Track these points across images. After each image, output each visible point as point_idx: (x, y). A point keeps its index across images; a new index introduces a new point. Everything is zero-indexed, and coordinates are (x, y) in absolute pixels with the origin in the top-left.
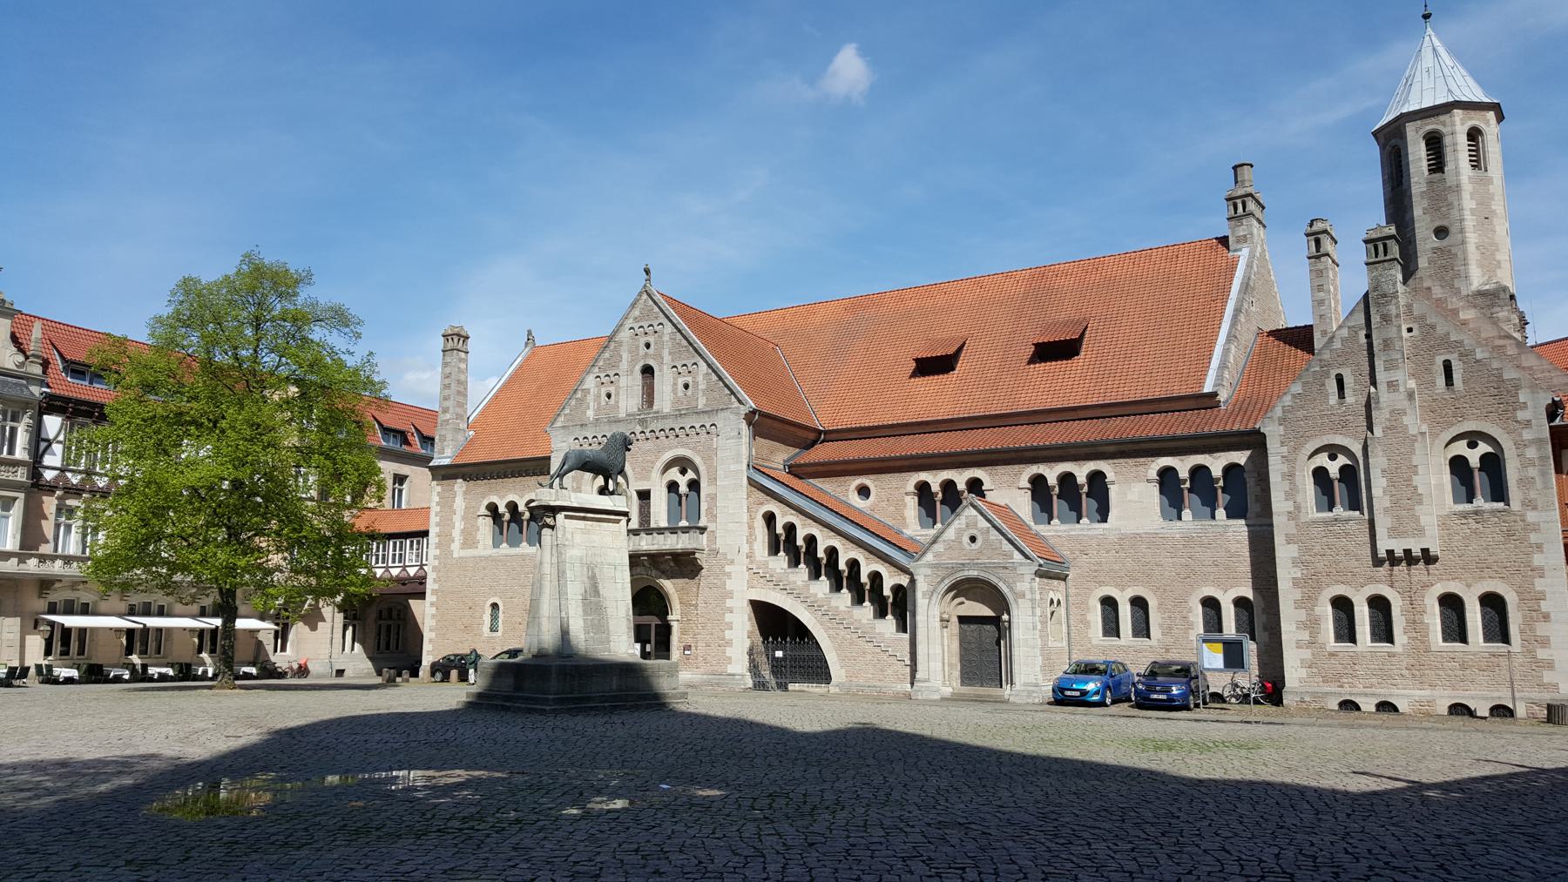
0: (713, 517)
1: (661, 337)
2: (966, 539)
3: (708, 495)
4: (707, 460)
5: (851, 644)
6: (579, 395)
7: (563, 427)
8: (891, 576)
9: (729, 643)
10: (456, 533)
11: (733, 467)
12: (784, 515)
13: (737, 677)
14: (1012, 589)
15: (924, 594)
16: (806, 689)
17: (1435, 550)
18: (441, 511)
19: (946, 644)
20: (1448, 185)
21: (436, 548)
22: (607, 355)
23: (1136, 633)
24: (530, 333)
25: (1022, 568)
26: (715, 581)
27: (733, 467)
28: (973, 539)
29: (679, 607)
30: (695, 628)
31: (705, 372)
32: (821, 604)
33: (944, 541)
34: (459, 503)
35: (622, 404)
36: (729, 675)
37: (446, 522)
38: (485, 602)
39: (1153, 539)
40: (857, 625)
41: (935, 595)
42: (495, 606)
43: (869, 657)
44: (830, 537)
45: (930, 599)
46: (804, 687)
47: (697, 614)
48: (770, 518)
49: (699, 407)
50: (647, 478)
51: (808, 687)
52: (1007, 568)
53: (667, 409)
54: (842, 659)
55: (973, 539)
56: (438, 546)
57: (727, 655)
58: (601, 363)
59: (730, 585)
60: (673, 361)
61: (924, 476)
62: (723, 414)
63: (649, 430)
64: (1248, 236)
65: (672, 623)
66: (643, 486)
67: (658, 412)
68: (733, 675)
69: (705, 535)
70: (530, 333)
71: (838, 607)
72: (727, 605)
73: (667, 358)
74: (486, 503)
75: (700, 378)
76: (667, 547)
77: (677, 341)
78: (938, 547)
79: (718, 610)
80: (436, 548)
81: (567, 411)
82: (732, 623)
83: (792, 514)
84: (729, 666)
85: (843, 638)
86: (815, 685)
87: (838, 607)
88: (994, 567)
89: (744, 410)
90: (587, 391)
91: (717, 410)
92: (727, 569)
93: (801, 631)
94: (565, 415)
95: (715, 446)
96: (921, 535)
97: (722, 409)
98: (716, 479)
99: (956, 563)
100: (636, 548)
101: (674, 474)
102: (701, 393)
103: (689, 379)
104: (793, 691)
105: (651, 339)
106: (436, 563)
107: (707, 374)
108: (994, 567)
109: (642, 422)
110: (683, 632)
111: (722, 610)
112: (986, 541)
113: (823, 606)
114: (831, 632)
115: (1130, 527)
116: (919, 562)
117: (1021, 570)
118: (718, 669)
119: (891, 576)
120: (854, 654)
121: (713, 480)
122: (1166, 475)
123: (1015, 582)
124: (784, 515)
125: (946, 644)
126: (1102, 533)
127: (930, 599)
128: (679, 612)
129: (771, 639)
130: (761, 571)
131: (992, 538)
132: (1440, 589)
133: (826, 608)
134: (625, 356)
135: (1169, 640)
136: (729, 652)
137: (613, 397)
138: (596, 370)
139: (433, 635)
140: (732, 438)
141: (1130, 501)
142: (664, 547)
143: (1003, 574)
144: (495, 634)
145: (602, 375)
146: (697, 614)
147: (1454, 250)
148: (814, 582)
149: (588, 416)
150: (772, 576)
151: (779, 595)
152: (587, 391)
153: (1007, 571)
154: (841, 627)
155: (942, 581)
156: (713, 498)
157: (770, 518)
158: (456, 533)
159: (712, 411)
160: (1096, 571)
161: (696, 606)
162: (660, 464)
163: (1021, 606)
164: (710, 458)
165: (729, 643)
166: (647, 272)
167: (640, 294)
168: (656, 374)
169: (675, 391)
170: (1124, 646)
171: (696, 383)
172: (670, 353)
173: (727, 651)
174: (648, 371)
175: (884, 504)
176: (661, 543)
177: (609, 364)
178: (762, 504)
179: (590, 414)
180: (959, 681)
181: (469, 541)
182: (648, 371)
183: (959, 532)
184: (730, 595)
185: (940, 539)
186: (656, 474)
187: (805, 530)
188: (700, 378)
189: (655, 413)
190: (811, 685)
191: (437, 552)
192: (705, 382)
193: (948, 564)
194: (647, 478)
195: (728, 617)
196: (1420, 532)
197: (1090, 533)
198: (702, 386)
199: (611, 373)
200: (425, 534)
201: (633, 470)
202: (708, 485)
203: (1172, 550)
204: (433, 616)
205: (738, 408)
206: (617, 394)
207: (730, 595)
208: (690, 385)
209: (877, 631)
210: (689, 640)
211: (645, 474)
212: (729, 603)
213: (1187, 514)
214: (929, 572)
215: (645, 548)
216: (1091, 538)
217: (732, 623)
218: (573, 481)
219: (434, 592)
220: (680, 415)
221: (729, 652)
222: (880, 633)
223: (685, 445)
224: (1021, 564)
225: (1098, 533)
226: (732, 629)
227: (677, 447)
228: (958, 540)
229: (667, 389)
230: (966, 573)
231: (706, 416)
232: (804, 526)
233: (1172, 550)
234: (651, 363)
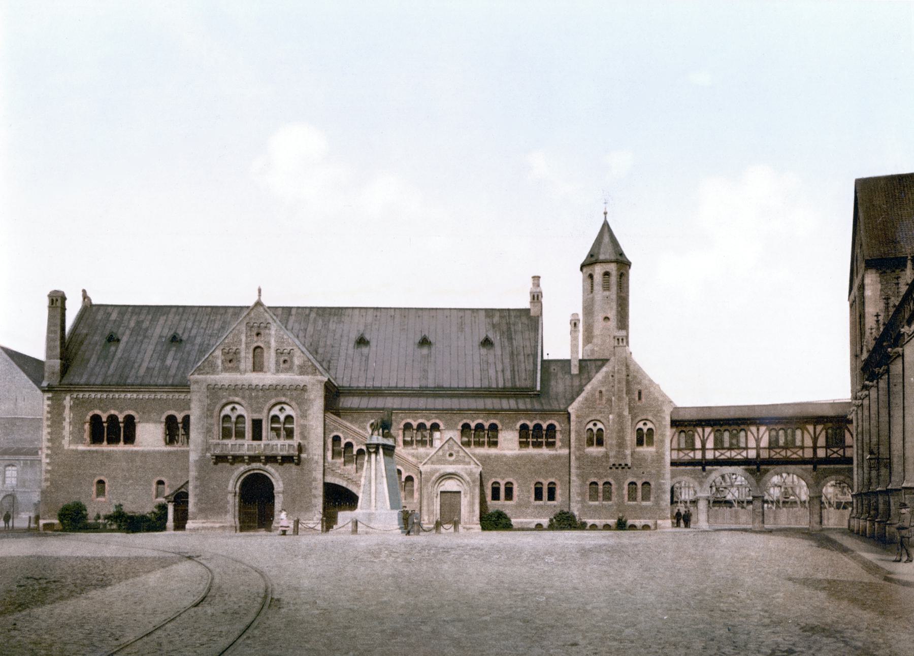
17: (630, 465)
24: (84, 291)
48: (336, 439)
66: (256, 416)
70: (84, 291)
74: (91, 414)
132: (630, 480)
162: (268, 406)
166: (260, 291)
186: (266, 411)
196: (625, 456)
207: (315, 480)
211: (260, 410)
228: (444, 455)
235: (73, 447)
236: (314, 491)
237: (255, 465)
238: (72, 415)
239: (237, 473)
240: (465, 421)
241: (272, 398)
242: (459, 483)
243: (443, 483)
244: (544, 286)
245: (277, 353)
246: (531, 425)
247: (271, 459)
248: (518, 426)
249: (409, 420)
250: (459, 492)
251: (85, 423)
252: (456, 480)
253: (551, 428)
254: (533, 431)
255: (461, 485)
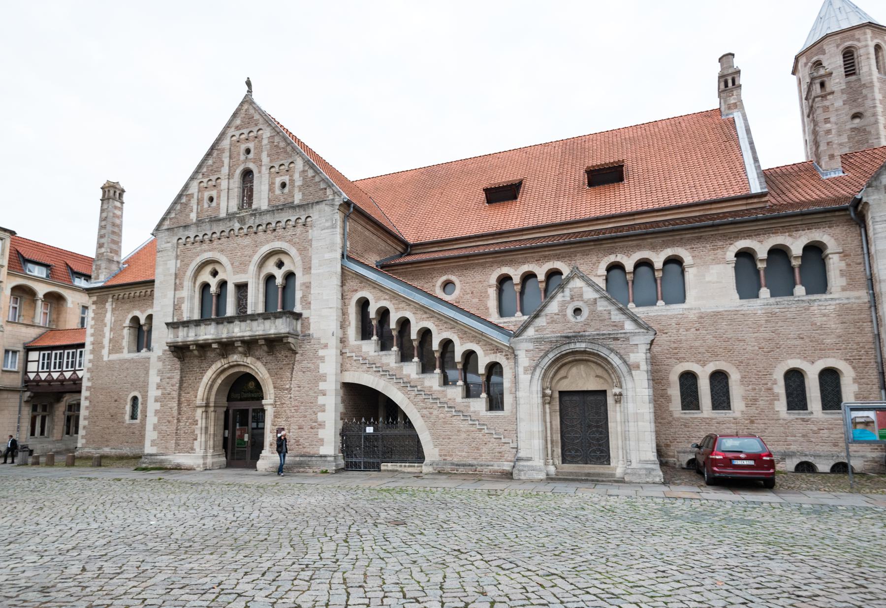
0: (307, 304)
1: (260, 142)
2: (570, 312)
3: (304, 284)
4: (304, 250)
5: (445, 423)
6: (184, 200)
7: (168, 229)
8: (486, 355)
9: (322, 425)
10: (106, 342)
11: (327, 256)
12: (377, 300)
13: (329, 459)
14: (625, 362)
15: (526, 370)
16: (399, 469)
18: (95, 324)
19: (548, 420)
20: (863, 83)
21: (91, 353)
22: (210, 162)
23: (715, 407)
25: (635, 338)
26: (309, 365)
27: (327, 256)
28: (577, 311)
29: (272, 391)
30: (288, 411)
31: (301, 169)
32: (414, 385)
33: (546, 315)
34: (109, 317)
35: (223, 205)
36: (321, 456)
37: (98, 333)
38: (127, 395)
39: (732, 317)
40: (451, 404)
41: (538, 371)
42: (135, 399)
43: (464, 435)
44: (423, 319)
45: (533, 374)
46: (397, 466)
47: (291, 398)
48: (364, 304)
49: (296, 203)
50: (245, 271)
51: (401, 466)
52: (616, 339)
53: (264, 206)
54: (435, 437)
55: (577, 311)
56: (93, 352)
57: (320, 436)
58: (205, 170)
59: (324, 368)
60: (271, 161)
61: (505, 270)
62: (318, 207)
63: (247, 226)
64: (738, 103)
65: (266, 407)
66: (241, 279)
67: (256, 210)
68: (325, 456)
69: (299, 322)
71: (431, 387)
72: (320, 388)
73: (265, 159)
75: (297, 176)
76: (261, 333)
77: (275, 144)
78: (541, 321)
79: (311, 393)
80: (91, 353)
81: (173, 215)
82: (324, 405)
83: (385, 299)
84: (321, 447)
85: (437, 416)
86: (407, 464)
87: (431, 387)
88: (603, 339)
89: (338, 201)
90: (192, 195)
91: (313, 203)
92: (321, 353)
93: (392, 410)
94: (171, 219)
95: (310, 238)
96: (505, 323)
97: (317, 203)
98: (310, 268)
99: (561, 337)
100: (230, 335)
101: (271, 267)
102: (296, 190)
103: (286, 179)
104: (385, 471)
105: (251, 145)
106: (90, 365)
107: (304, 171)
108: (603, 339)
109: (242, 220)
110: (276, 416)
111: (315, 393)
112: (592, 312)
113: (416, 386)
114: (425, 412)
115: (710, 306)
116: (520, 338)
117: (634, 340)
118: (311, 451)
119: (486, 355)
120: (449, 433)
121: (307, 269)
122: (746, 255)
123: (627, 354)
124: (377, 300)
125: (548, 420)
126: (681, 312)
127: (533, 374)
128: (273, 396)
129: (363, 420)
130: (354, 354)
131: (600, 309)
133: (419, 388)
134: (226, 161)
135: (753, 411)
136: (322, 433)
137: (215, 200)
138: (200, 176)
139: (86, 423)
140: (327, 228)
141: (709, 282)
142: (257, 333)
143: (613, 344)
144: (134, 421)
145: (205, 180)
146: (291, 398)
147: (868, 129)
148: (406, 364)
149: (191, 218)
150: (364, 359)
151: (372, 377)
152: (192, 195)
153: (619, 342)
154: (435, 406)
155: (546, 355)
156: (307, 286)
157: (364, 304)
158: (106, 342)
159: (308, 204)
160: (676, 348)
161: (290, 389)
162: (256, 258)
163: (635, 378)
164: (305, 249)
165: (322, 425)
167: (242, 104)
168: (256, 174)
169: (271, 189)
170: (708, 418)
171: (292, 181)
172: (269, 155)
173: (319, 433)
174: (247, 174)
175: (468, 296)
176: (254, 329)
177: (212, 170)
178: (356, 291)
179: (193, 216)
180: (560, 459)
181: (115, 348)
182: (247, 174)
183: (564, 305)
184: (323, 378)
185: (543, 313)
186: (252, 268)
187: (398, 313)
188: (297, 176)
189: (253, 210)
190: (403, 464)
191: (91, 357)
192: (302, 178)
193: (552, 337)
194: (245, 271)
195: (321, 400)
197: (669, 313)
198: (298, 182)
199: (214, 178)
200: (82, 345)
201: (232, 264)
202: (303, 275)
203: (755, 326)
204: (87, 408)
205: (333, 200)
206: (219, 197)
207: (323, 378)
208: (287, 183)
209: (472, 409)
210: (282, 423)
211: (242, 267)
212: (322, 386)
213: (765, 292)
214: (531, 346)
215: (239, 334)
216: (670, 318)
217: (324, 405)
218: (176, 278)
219: (88, 388)
220: (276, 209)
221: (322, 433)
222: (475, 412)
223: (280, 238)
224: (635, 334)
225: (676, 313)
226: (324, 411)
227: (273, 241)
228: (562, 312)
229: (265, 188)
230: (572, 346)
231: (302, 210)
232: (397, 309)
233: (755, 326)
234: (251, 166)
235: (114, 357)
236: (321, 400)
237: (235, 358)
238: (113, 318)
239: (210, 374)
240: (612, 258)
241: (262, 244)
242: (599, 371)
243: (562, 373)
244: (737, 63)
245: (270, 173)
246: (761, 248)
247: (250, 345)
248: (731, 255)
249: (505, 270)
250: (604, 392)
251: (124, 327)
252: (592, 365)
253: (815, 250)
254: (768, 260)
255: (606, 376)
